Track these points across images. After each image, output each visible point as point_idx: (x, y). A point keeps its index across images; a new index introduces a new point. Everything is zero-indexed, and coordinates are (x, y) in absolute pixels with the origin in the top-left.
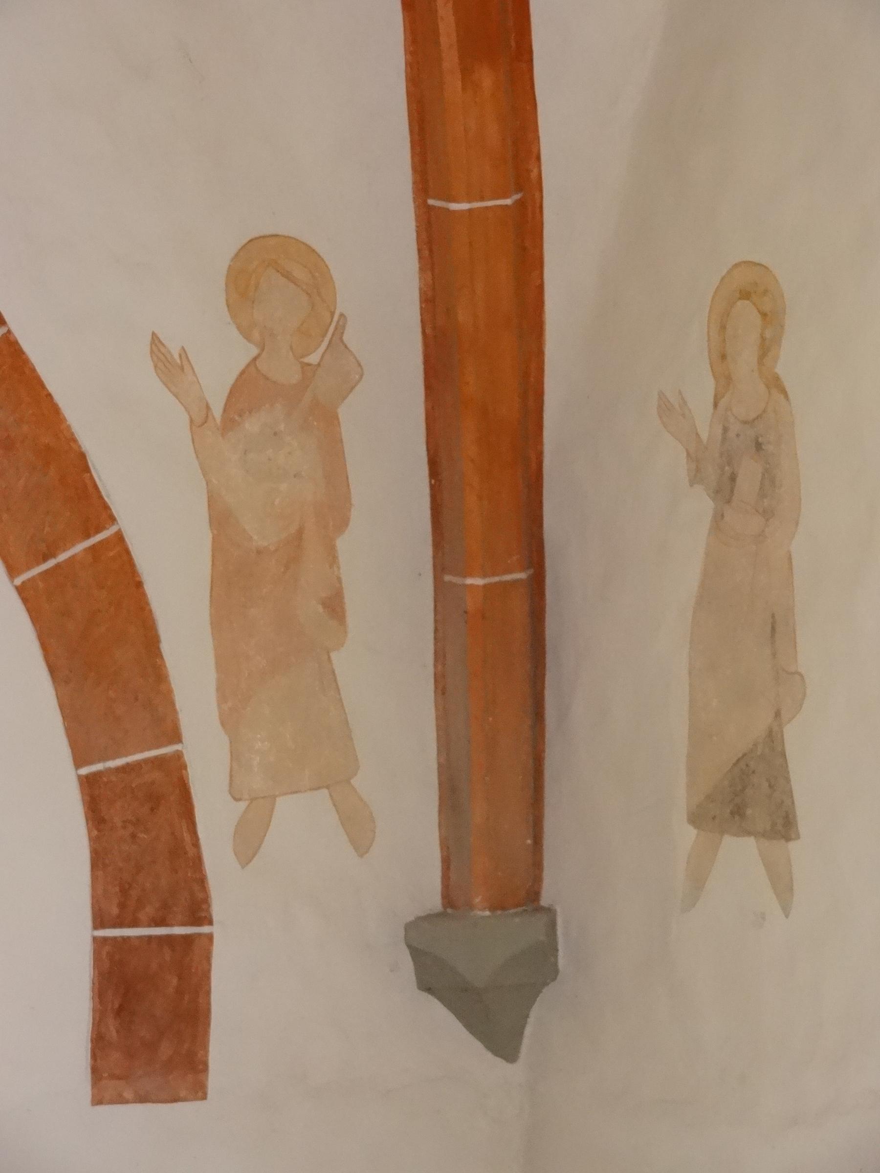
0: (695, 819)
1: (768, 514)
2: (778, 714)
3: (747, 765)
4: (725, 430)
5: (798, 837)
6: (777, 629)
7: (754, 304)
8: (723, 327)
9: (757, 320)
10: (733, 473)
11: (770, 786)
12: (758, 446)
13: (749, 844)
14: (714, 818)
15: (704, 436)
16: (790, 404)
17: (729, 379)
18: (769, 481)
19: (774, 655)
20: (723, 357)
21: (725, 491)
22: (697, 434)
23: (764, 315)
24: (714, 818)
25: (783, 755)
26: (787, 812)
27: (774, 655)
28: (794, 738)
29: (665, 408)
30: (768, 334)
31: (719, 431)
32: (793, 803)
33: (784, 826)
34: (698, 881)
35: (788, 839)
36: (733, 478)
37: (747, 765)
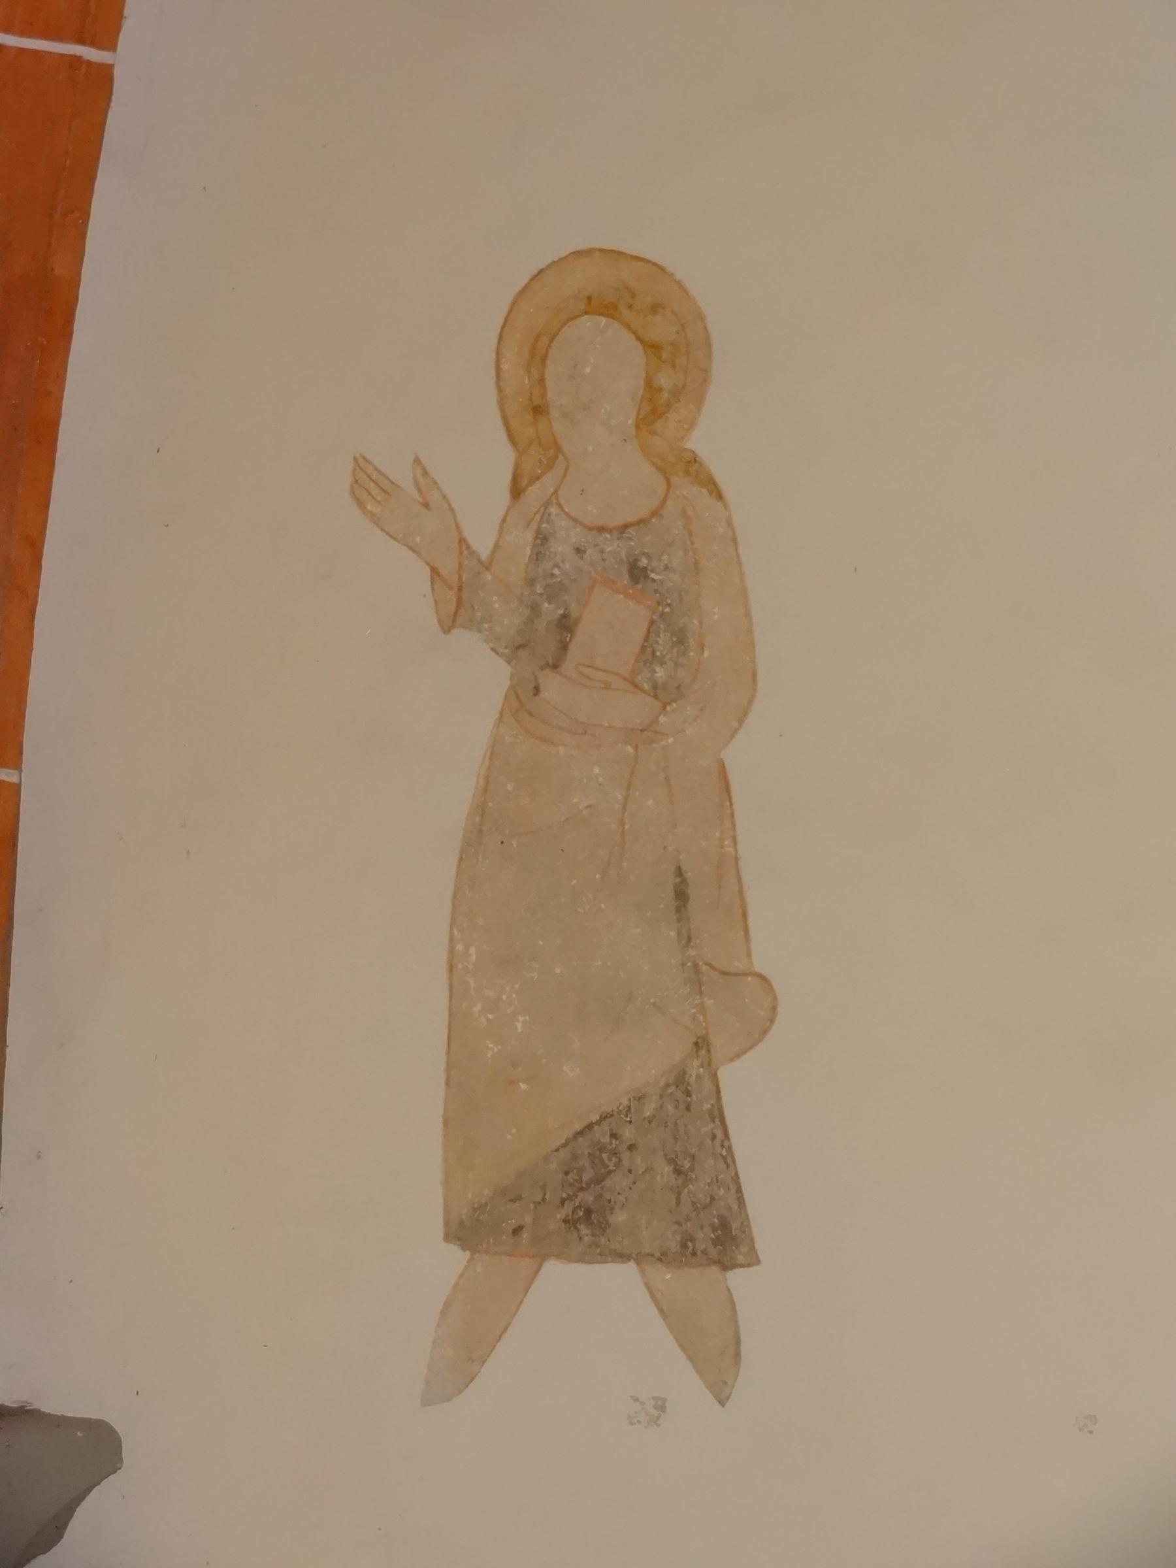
0: (465, 1231)
1: (665, 695)
2: (701, 1044)
3: (614, 1136)
4: (542, 539)
5: (754, 1260)
6: (693, 896)
7: (628, 326)
8: (537, 357)
9: (638, 355)
10: (565, 616)
11: (678, 1171)
12: (637, 573)
13: (622, 1277)
14: (517, 1231)
15: (483, 545)
16: (725, 505)
17: (553, 451)
18: (670, 632)
19: (687, 941)
20: (539, 410)
21: (545, 641)
22: (462, 541)
23: (652, 348)
24: (517, 1231)
25: (717, 1115)
26: (720, 1217)
27: (687, 941)
28: (742, 1085)
29: (368, 486)
30: (665, 380)
31: (525, 539)
32: (741, 1201)
33: (722, 1240)
34: (469, 1342)
35: (726, 1265)
36: (566, 625)
37: (614, 1136)
